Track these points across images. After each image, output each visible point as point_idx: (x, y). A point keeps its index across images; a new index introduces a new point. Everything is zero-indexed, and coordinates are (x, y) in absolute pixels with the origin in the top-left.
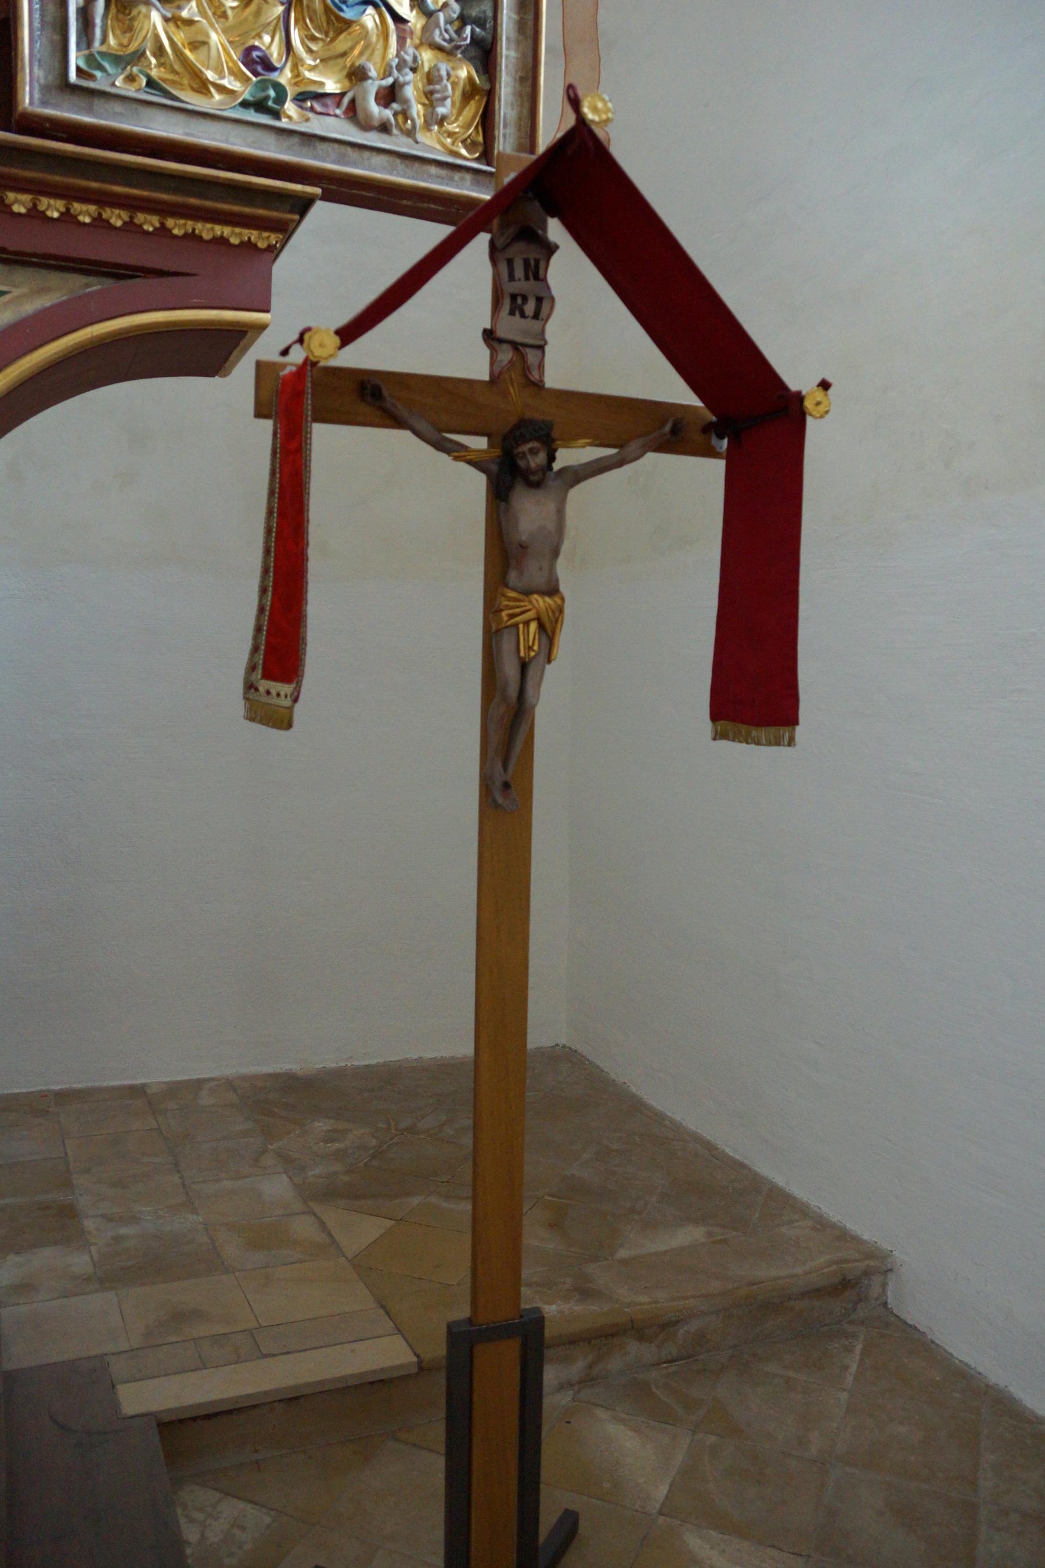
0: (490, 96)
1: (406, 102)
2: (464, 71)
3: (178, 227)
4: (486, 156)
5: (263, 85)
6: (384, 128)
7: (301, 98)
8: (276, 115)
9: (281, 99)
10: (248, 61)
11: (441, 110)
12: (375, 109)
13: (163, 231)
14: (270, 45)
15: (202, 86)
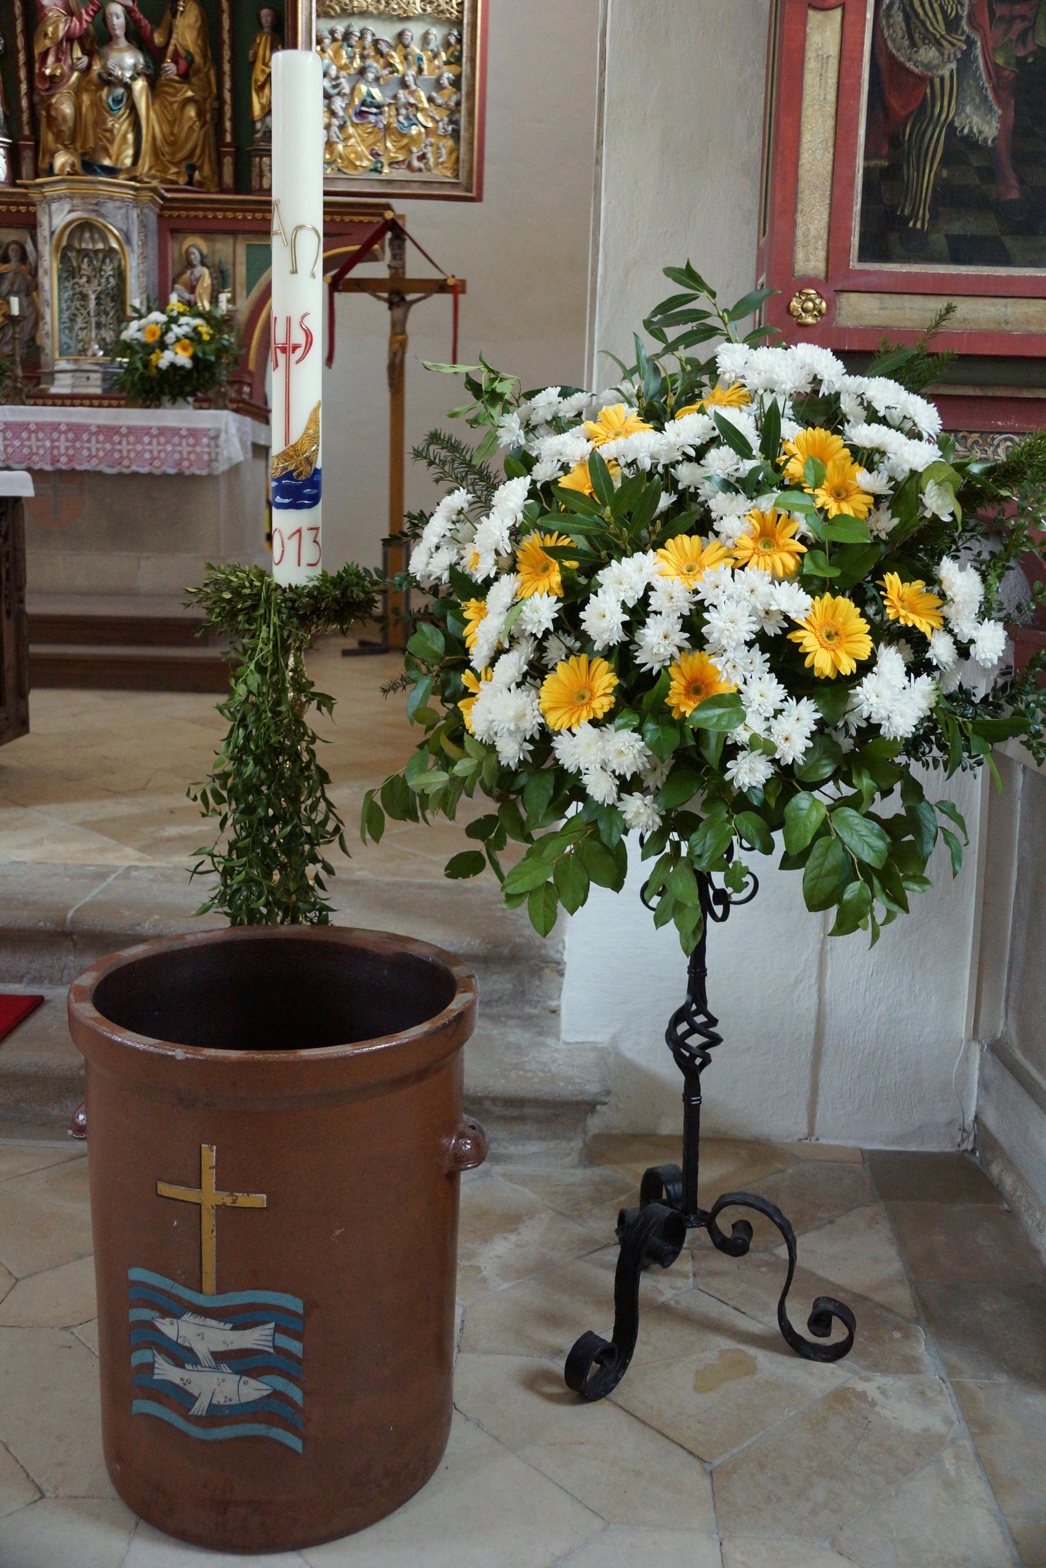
0: (458, 150)
1: (428, 159)
2: (450, 143)
3: (347, 219)
4: (457, 176)
5: (377, 162)
6: (420, 170)
7: (390, 164)
8: (380, 172)
9: (382, 167)
10: (372, 155)
11: (441, 160)
12: (416, 164)
13: (342, 221)
14: (379, 148)
15: (356, 167)
